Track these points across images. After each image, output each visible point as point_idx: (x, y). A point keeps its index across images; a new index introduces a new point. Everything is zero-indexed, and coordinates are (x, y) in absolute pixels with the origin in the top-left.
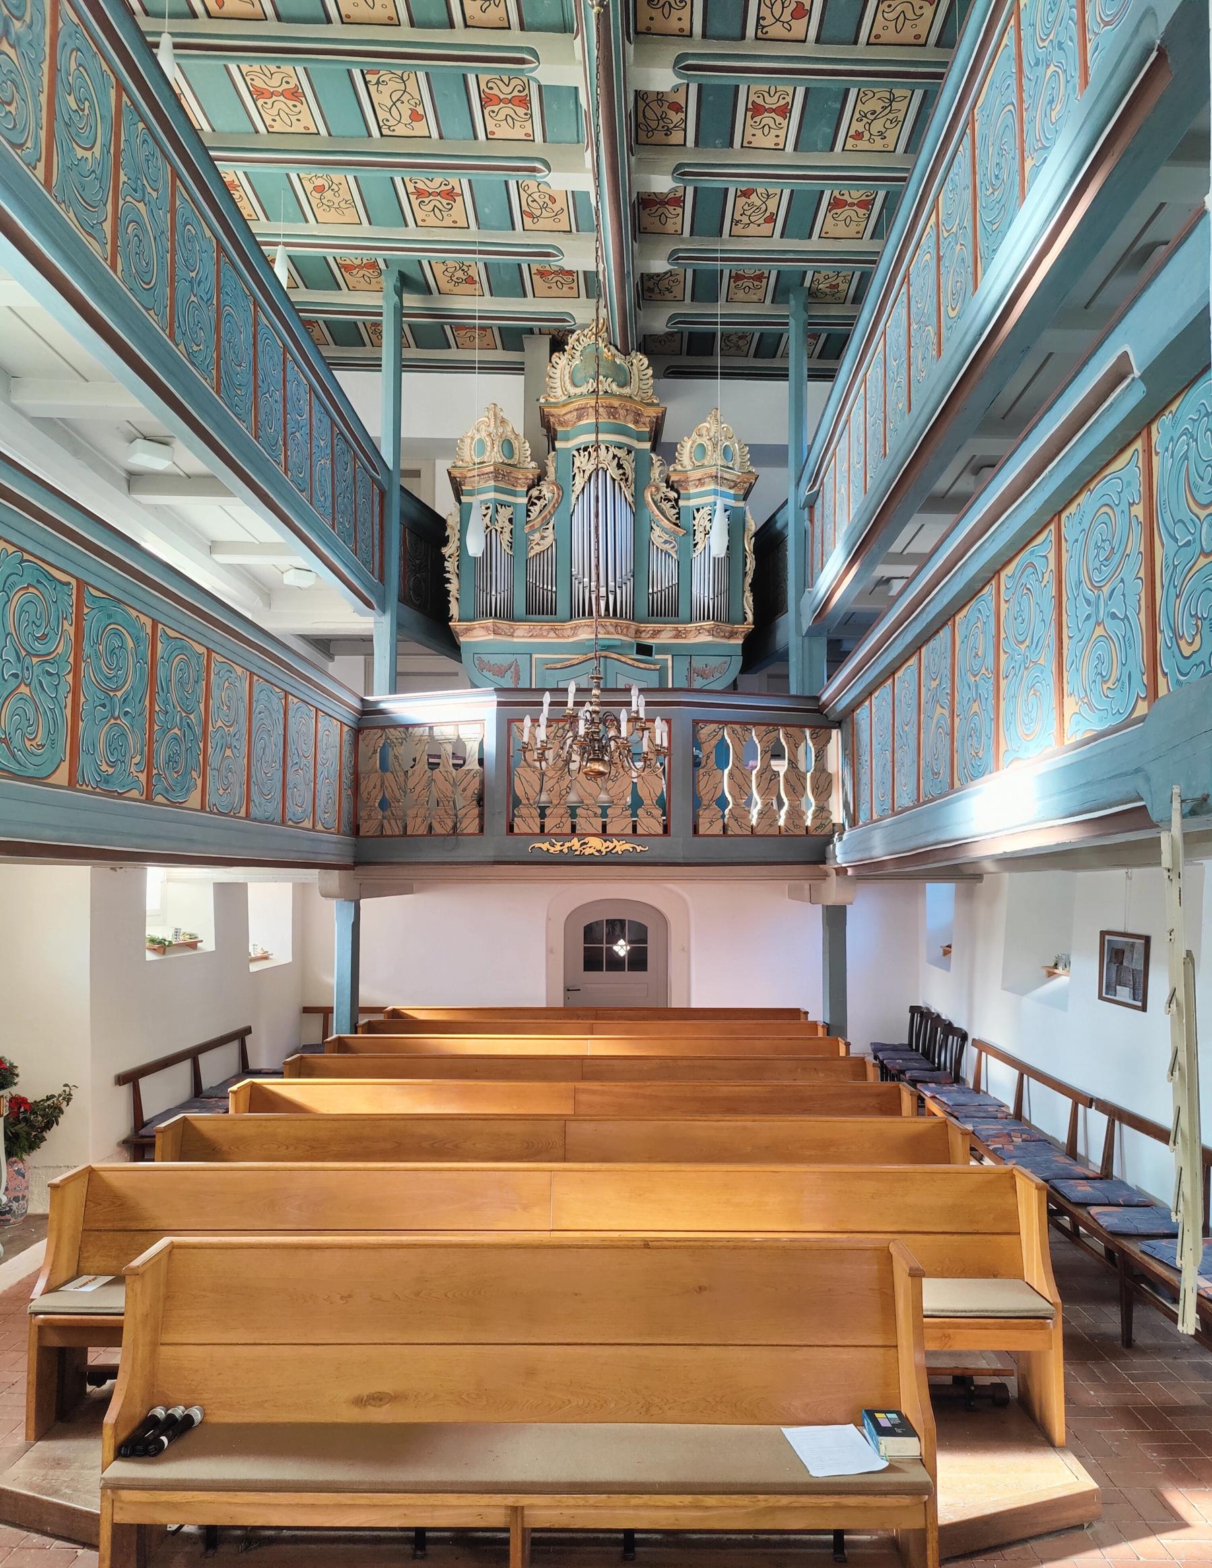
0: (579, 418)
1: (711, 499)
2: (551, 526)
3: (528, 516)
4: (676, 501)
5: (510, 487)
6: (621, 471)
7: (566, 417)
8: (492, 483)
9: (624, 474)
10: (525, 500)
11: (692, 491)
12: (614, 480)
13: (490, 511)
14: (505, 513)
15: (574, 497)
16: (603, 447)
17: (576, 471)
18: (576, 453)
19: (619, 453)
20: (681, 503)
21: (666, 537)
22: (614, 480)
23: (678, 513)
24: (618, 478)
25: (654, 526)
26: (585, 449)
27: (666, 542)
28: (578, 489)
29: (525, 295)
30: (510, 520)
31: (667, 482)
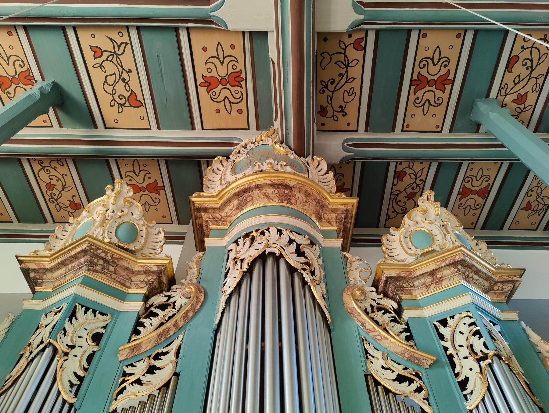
0: (240, 207)
1: (467, 299)
2: (174, 347)
3: (136, 332)
4: (399, 312)
5: (120, 287)
6: (302, 259)
7: (223, 214)
8: (83, 272)
9: (308, 264)
10: (137, 307)
11: (420, 294)
12: (292, 270)
13: (58, 316)
14: (89, 323)
15: (224, 299)
16: (273, 230)
17: (231, 264)
18: (233, 246)
19: (299, 239)
20: (407, 315)
21: (399, 370)
22: (292, 270)
23: (407, 330)
24: (299, 267)
25: (371, 350)
26: (247, 235)
27: (400, 379)
28: (231, 282)
29: (193, 128)
30: (97, 338)
31: (375, 284)
